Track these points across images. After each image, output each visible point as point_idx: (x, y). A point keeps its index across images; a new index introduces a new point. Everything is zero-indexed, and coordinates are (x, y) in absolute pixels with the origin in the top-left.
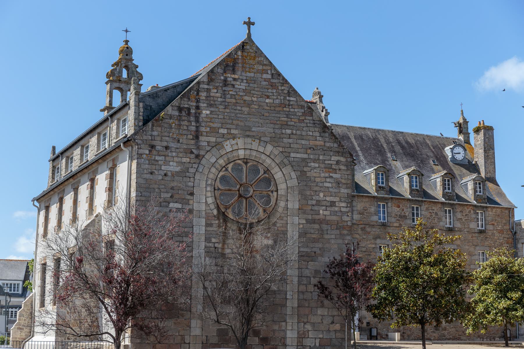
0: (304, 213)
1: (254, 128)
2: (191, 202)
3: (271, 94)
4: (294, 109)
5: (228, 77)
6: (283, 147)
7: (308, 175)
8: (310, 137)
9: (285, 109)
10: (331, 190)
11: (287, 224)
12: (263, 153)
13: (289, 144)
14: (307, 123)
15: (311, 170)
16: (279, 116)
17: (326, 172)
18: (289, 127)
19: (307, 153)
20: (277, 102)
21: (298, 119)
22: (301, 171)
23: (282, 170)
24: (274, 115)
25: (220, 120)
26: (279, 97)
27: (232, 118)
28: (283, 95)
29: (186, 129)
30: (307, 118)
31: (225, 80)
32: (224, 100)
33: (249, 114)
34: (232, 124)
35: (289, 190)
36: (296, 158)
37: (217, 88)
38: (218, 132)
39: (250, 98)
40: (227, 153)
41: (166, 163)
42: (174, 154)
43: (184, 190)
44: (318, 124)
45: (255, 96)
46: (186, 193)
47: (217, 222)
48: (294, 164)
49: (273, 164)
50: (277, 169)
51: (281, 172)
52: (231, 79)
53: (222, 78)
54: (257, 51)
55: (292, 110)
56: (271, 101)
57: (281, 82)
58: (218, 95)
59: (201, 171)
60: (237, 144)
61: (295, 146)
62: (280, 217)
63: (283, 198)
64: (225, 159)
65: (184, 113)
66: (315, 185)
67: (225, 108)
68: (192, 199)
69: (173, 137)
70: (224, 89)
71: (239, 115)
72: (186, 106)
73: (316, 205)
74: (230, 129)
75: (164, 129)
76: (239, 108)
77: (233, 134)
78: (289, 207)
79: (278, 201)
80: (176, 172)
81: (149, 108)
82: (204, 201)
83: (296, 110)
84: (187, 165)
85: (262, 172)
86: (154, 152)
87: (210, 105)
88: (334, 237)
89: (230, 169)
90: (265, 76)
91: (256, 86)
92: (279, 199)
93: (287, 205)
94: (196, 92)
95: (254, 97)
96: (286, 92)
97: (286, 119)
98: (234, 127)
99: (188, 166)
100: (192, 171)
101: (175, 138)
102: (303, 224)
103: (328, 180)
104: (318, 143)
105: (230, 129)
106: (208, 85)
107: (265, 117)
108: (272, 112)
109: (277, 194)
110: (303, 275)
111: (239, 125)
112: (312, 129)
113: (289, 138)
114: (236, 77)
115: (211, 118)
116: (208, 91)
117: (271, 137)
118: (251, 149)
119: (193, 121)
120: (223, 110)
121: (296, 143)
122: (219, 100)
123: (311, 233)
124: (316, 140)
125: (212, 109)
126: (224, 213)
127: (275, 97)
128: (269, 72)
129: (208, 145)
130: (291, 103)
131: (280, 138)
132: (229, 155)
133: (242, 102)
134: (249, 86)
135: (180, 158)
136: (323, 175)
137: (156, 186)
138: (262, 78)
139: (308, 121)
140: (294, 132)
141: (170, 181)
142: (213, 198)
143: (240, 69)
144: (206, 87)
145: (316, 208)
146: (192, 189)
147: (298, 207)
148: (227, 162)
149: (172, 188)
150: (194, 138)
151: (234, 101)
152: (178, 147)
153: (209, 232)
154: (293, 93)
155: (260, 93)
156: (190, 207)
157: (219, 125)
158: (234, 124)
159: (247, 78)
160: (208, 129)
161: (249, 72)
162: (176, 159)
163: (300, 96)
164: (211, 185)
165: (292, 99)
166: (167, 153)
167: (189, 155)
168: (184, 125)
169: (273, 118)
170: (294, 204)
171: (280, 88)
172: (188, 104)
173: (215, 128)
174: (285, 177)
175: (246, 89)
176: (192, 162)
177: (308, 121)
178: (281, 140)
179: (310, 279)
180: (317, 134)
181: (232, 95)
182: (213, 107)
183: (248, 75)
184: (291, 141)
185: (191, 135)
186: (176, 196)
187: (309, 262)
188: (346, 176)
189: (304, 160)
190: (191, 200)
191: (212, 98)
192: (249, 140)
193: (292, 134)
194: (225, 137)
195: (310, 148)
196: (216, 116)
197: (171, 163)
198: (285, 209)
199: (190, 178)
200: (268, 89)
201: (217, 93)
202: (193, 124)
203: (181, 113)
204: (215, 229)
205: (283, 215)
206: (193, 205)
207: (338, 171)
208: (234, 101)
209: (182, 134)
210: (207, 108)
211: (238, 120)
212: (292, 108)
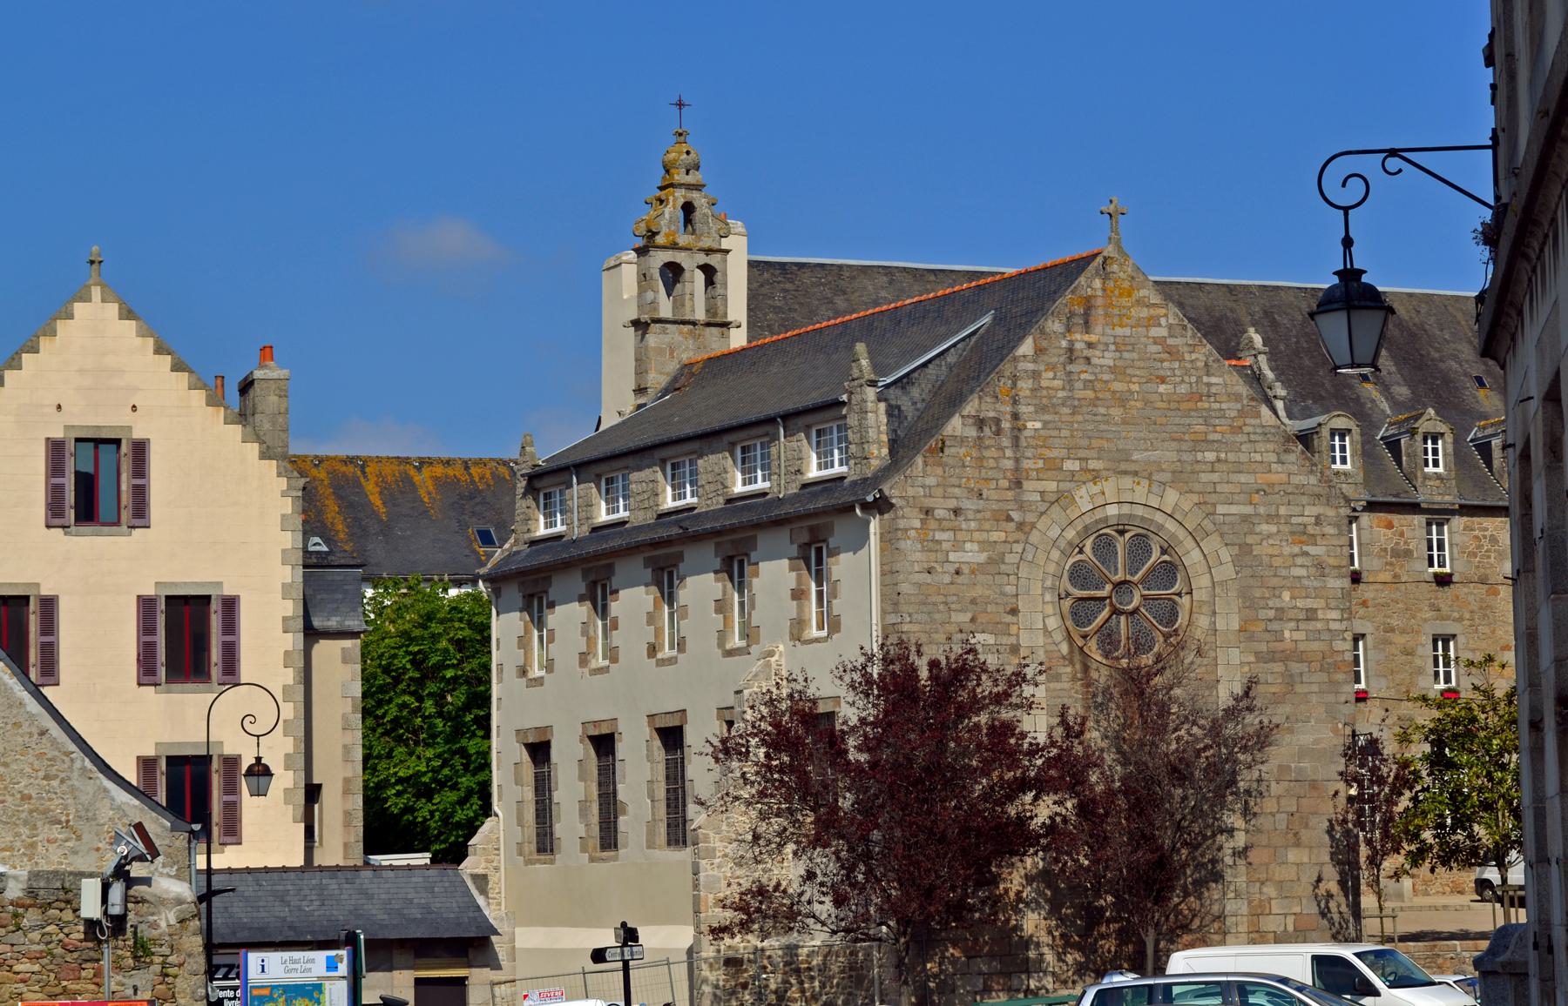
0: (1251, 638)
2: (1014, 629)
10: (1306, 582)
11: (1216, 665)
15: (1262, 540)
16: (1187, 421)
17: (1294, 543)
19: (1251, 504)
20: (1183, 391)
24: (1177, 420)
26: (1186, 379)
27: (1090, 434)
30: (1248, 421)
31: (1071, 350)
33: (1125, 422)
34: (1089, 448)
35: (1218, 590)
36: (1229, 515)
41: (958, 546)
45: (1134, 380)
46: (1001, 609)
47: (1069, 669)
48: (1225, 529)
49: (1181, 534)
50: (1189, 543)
51: (1198, 549)
53: (1064, 344)
55: (1216, 406)
57: (1190, 342)
58: (1057, 383)
59: (1030, 558)
60: (1103, 493)
63: (1205, 609)
67: (1073, 414)
71: (1103, 427)
72: (992, 414)
73: (1275, 619)
76: (1102, 410)
77: (1093, 470)
79: (1195, 616)
80: (978, 564)
81: (896, 412)
83: (1224, 406)
84: (1001, 548)
86: (932, 524)
87: (1041, 409)
88: (1317, 690)
91: (1135, 355)
92: (1194, 609)
96: (1200, 364)
97: (1203, 428)
99: (1002, 550)
101: (973, 490)
102: (1249, 663)
103: (1299, 561)
104: (1273, 478)
106: (1035, 361)
112: (1261, 447)
113: (1213, 471)
114: (1093, 338)
116: (1036, 375)
117: (1173, 472)
119: (1007, 447)
120: (1069, 418)
121: (1228, 482)
122: (1061, 394)
125: (1047, 417)
126: (1081, 649)
128: (1163, 321)
129: (1043, 501)
130: (1214, 390)
131: (1193, 472)
134: (1120, 358)
136: (1287, 550)
137: (941, 599)
138: (1148, 338)
140: (1223, 456)
142: (1059, 617)
143: (1101, 320)
144: (1031, 366)
145: (1275, 626)
149: (973, 601)
150: (1013, 486)
151: (1090, 394)
152: (981, 508)
153: (1055, 693)
156: (1013, 640)
157: (1064, 453)
159: (1117, 340)
160: (1040, 464)
161: (1121, 326)
162: (976, 535)
165: (1213, 380)
167: (1004, 524)
170: (1229, 621)
171: (1187, 357)
173: (1055, 459)
176: (1010, 539)
180: (1273, 457)
181: (1086, 381)
184: (1215, 477)
185: (1005, 478)
186: (982, 619)
188: (1339, 549)
189: (1245, 518)
192: (1127, 482)
193: (1219, 460)
195: (1257, 492)
196: (1055, 433)
197: (968, 546)
202: (1009, 453)
203: (982, 431)
204: (1066, 686)
206: (1018, 635)
207: (1318, 538)
208: (1090, 394)
209: (986, 479)
212: (1215, 402)
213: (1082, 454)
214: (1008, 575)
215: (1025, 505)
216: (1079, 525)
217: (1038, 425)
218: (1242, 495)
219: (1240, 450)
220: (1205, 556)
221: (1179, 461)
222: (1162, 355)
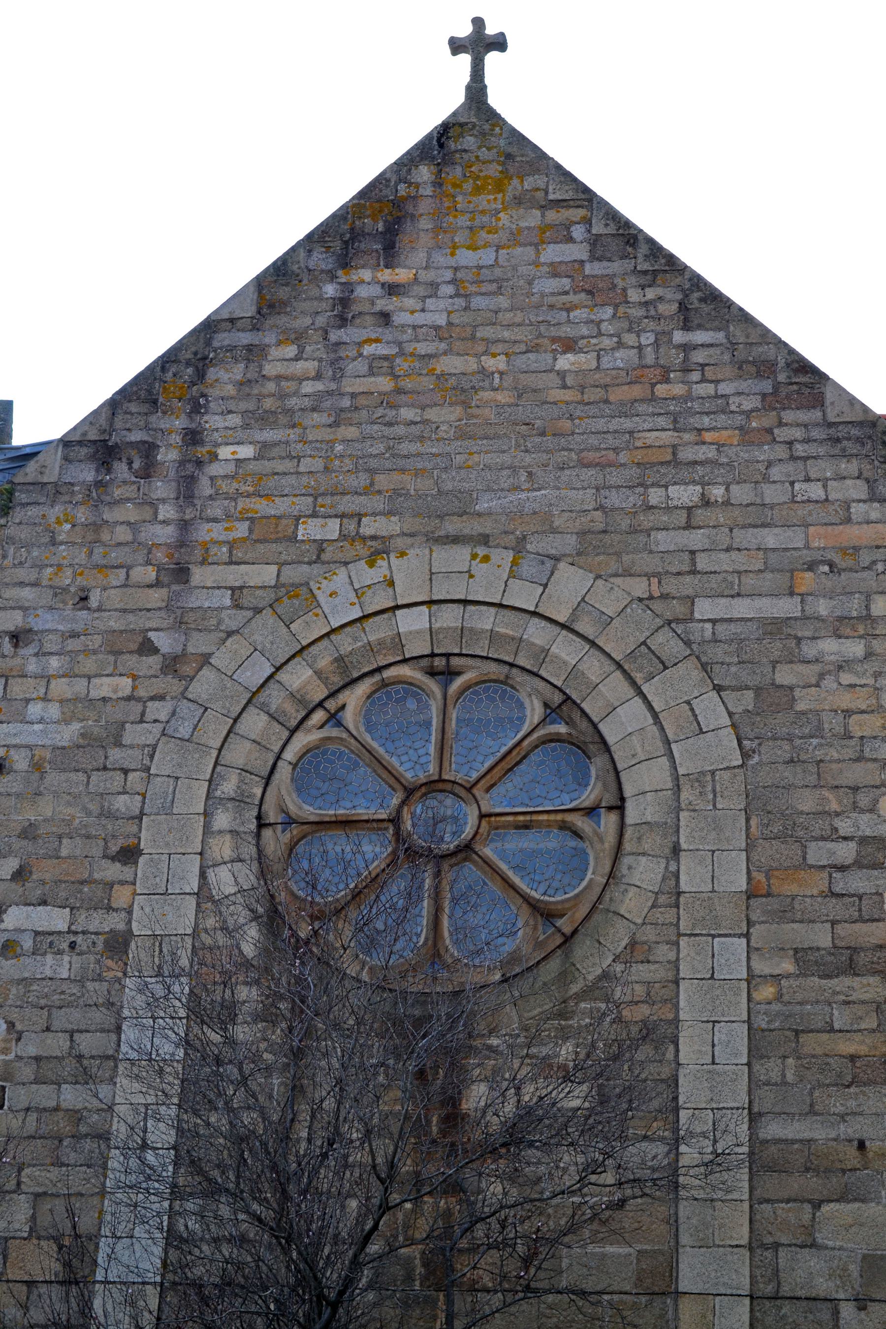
1: (487, 496)
3: (585, 331)
4: (717, 382)
5: (362, 282)
6: (648, 576)
7: (801, 706)
8: (811, 506)
9: (661, 390)
11: (677, 983)
12: (534, 614)
13: (686, 556)
14: (790, 443)
15: (822, 676)
16: (628, 424)
18: (684, 474)
19: (792, 594)
21: (741, 428)
22: (758, 690)
23: (645, 688)
24: (600, 424)
25: (305, 479)
26: (630, 339)
27: (373, 463)
28: (652, 325)
29: (130, 538)
30: (789, 416)
31: (344, 302)
32: (333, 386)
33: (462, 435)
34: (368, 491)
35: (686, 795)
36: (730, 620)
37: (299, 338)
38: (293, 539)
39: (472, 360)
40: (333, 631)
42: (54, 663)
43: (88, 837)
44: (859, 440)
45: (499, 348)
46: (96, 851)
48: (717, 653)
51: (638, 700)
52: (377, 290)
53: (330, 290)
54: (513, 150)
56: (586, 360)
57: (646, 266)
58: (309, 366)
59: (184, 731)
60: (391, 583)
61: (725, 562)
62: (633, 944)
63: (653, 842)
64: (324, 662)
65: (121, 469)
66: (850, 753)
67: (336, 424)
68: (130, 878)
69: (57, 582)
70: (334, 336)
71: (406, 447)
72: (136, 436)
73: (858, 864)
74: (359, 516)
75: (17, 549)
76: (407, 414)
77: (374, 538)
78: (684, 887)
79: (626, 861)
80: (55, 748)
82: (194, 884)
83: (725, 388)
84: (114, 713)
85: (534, 712)
89: (349, 717)
90: (552, 253)
91: (503, 301)
92: (628, 846)
93: (677, 875)
94: (190, 371)
95: (494, 355)
96: (669, 309)
97: (667, 437)
98: (378, 503)
99: (120, 717)
100: (142, 740)
101: (65, 590)
104: (853, 534)
105: (359, 516)
107: (549, 441)
108: (593, 410)
109: (622, 825)
110: (785, 1290)
111: (407, 495)
113: (688, 526)
114: (402, 275)
115: (261, 476)
117: (582, 534)
118: (465, 602)
119: (163, 501)
120: (325, 434)
122: (308, 387)
123: (832, 1030)
124: (848, 520)
125: (269, 435)
127: (607, 342)
128: (578, 232)
129: (237, 606)
130: (699, 357)
131: (634, 531)
132: (346, 643)
133: (428, 383)
134: (467, 308)
135: (84, 682)
139: (798, 433)
140: (717, 492)
141: (18, 795)
143: (425, 239)
146: (135, 829)
147: (742, 884)
148: (337, 681)
149: (28, 833)
150: (165, 580)
151: (384, 383)
152: (79, 627)
154: (706, 308)
155: (523, 334)
156: (116, 922)
158: (379, 492)
159: (459, 275)
160: (242, 530)
161: (474, 248)
162: (60, 687)
163: (745, 318)
164: (239, 800)
165: (700, 337)
166: (18, 661)
167: (131, 661)
168: (116, 523)
169: (593, 441)
171: (634, 295)
172: (147, 428)
173: (279, 517)
174: (662, 729)
175: (450, 324)
176: (142, 693)
177: (798, 433)
178: (642, 538)
179: (836, 1313)
180: (857, 490)
181: (374, 358)
182: (274, 425)
183: (463, 262)
184: (696, 539)
185: (148, 563)
186: (45, 871)
187: (826, 1208)
190: (122, 883)
191: (271, 387)
192: (460, 556)
193: (706, 502)
194: (325, 557)
195: (811, 567)
196: (288, 465)
198: (662, 899)
199: (126, 772)
200: (568, 310)
201: (297, 359)
202: (167, 512)
203: (109, 471)
205: (649, 934)
208: (384, 383)
209: (101, 568)
210: (240, 434)
211: (403, 471)
212: (703, 380)
213: (347, 504)
214: (126, 772)
215: (190, 617)
216: (324, 656)
217: (246, 451)
218: (769, 576)
219: (766, 478)
220: (655, 715)
221: (601, 508)
222: (571, 297)
